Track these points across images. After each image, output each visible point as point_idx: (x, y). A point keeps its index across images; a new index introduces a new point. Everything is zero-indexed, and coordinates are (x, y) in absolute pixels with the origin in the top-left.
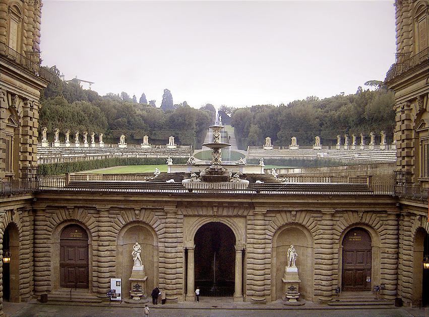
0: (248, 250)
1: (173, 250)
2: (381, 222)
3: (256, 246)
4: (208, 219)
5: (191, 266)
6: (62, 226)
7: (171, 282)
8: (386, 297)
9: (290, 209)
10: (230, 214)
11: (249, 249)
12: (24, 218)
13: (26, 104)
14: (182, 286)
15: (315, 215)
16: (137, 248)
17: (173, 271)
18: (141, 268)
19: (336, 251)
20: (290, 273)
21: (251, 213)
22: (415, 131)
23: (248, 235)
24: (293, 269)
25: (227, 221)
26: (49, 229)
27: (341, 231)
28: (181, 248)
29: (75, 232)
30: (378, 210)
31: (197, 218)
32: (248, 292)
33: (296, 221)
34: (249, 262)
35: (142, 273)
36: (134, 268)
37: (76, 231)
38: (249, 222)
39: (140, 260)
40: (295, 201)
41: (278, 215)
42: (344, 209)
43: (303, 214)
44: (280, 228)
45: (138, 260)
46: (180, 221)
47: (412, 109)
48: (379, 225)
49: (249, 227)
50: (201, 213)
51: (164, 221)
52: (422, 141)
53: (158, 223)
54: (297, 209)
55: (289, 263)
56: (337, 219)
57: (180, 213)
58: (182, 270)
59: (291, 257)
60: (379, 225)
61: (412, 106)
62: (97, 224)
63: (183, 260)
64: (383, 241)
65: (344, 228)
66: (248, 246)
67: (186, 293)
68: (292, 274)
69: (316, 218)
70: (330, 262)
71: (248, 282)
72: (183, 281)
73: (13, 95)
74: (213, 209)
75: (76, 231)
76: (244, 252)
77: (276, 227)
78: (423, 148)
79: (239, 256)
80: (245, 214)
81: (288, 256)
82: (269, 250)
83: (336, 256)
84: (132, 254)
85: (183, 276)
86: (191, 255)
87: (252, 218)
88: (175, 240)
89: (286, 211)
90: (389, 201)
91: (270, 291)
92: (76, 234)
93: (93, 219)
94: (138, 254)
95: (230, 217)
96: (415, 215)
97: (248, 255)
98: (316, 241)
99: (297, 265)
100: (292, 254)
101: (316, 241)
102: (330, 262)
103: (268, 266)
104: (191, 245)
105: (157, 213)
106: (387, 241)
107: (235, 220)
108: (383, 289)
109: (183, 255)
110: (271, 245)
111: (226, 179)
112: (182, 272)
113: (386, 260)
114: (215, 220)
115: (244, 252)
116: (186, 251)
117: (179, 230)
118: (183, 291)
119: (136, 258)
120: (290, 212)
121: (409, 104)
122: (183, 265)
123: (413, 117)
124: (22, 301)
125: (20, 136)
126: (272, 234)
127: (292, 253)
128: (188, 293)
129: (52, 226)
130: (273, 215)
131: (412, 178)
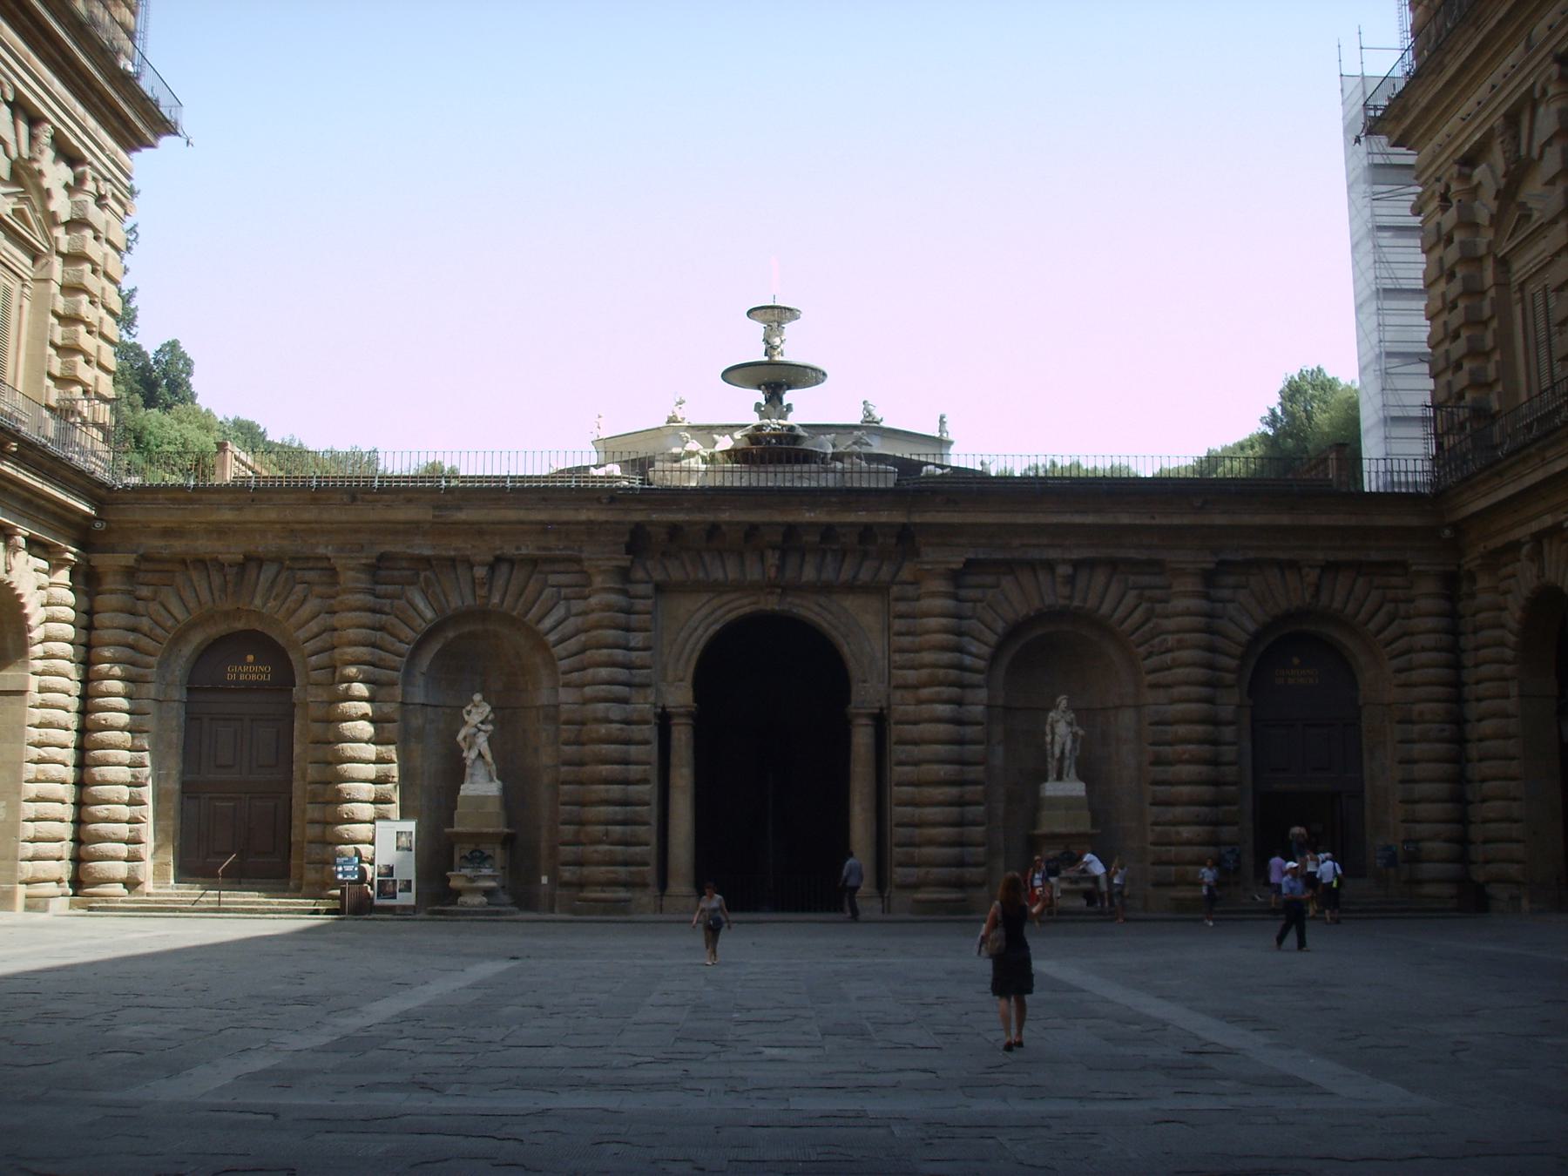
0: (899, 711)
1: (616, 711)
2: (1388, 607)
3: (925, 692)
4: (746, 601)
5: (682, 777)
6: (197, 639)
7: (607, 833)
8: (1429, 889)
9: (1053, 554)
10: (828, 574)
11: (904, 707)
12: (53, 590)
13: (80, 180)
14: (649, 851)
15: (1145, 580)
16: (478, 713)
17: (616, 791)
18: (493, 789)
19: (1226, 712)
20: (1056, 802)
21: (905, 575)
22: (1495, 256)
23: (897, 657)
24: (1074, 788)
25: (817, 609)
26: (145, 642)
27: (1244, 637)
28: (643, 705)
29: (244, 662)
30: (1375, 556)
31: (705, 597)
32: (898, 874)
33: (1076, 603)
34: (903, 757)
35: (494, 808)
36: (467, 789)
37: (250, 658)
38: (902, 607)
39: (489, 757)
40: (1067, 519)
41: (1007, 582)
42: (1251, 555)
43: (1100, 578)
44: (1016, 630)
45: (479, 763)
46: (640, 605)
47: (1480, 183)
48: (1380, 618)
49: (899, 625)
50: (720, 575)
51: (578, 606)
52: (1522, 287)
53: (559, 612)
54: (1076, 555)
55: (1052, 765)
56: (1226, 593)
57: (639, 574)
58: (648, 791)
59: (1057, 738)
60: (1380, 618)
61: (1480, 173)
62: (325, 620)
63: (651, 751)
64: (1403, 677)
65: (1251, 627)
66: (898, 694)
67: (663, 883)
68: (1068, 803)
69: (1147, 593)
70: (1205, 751)
71: (900, 833)
72: (649, 833)
73: (34, 120)
74: (762, 558)
75: (250, 658)
76: (880, 721)
77: (1000, 626)
78: (1529, 307)
79: (862, 738)
80: (885, 573)
81: (1048, 739)
82: (977, 711)
83: (1228, 733)
84: (460, 737)
85: (650, 812)
86: (682, 736)
87: (910, 591)
88: (622, 674)
89: (1032, 566)
90: (1414, 521)
91: (982, 870)
92: (250, 670)
93: (312, 605)
94: (482, 740)
95: (825, 589)
96: (1515, 546)
97: (895, 731)
98: (1151, 678)
99: (1082, 776)
100: (1061, 730)
101: (1151, 678)
102: (1205, 751)
103: (976, 772)
104: (680, 696)
105: (552, 579)
106: (1415, 676)
107: (850, 603)
108: (1414, 858)
109: (650, 731)
110: (982, 694)
111: (808, 457)
112: (647, 798)
113: (1417, 749)
114: (771, 603)
115: (880, 721)
116: (664, 720)
117: (637, 639)
118: (650, 872)
119: (473, 754)
120: (1050, 566)
121: (1466, 170)
122: (652, 771)
123: (1485, 208)
124: (28, 908)
125: (55, 289)
126: (985, 650)
127: (1062, 729)
128: (671, 882)
129: (159, 631)
130: (990, 580)
131: (1496, 429)
